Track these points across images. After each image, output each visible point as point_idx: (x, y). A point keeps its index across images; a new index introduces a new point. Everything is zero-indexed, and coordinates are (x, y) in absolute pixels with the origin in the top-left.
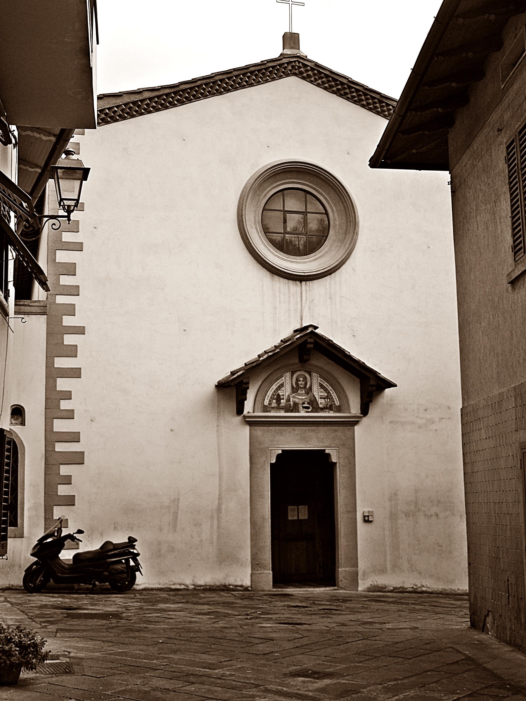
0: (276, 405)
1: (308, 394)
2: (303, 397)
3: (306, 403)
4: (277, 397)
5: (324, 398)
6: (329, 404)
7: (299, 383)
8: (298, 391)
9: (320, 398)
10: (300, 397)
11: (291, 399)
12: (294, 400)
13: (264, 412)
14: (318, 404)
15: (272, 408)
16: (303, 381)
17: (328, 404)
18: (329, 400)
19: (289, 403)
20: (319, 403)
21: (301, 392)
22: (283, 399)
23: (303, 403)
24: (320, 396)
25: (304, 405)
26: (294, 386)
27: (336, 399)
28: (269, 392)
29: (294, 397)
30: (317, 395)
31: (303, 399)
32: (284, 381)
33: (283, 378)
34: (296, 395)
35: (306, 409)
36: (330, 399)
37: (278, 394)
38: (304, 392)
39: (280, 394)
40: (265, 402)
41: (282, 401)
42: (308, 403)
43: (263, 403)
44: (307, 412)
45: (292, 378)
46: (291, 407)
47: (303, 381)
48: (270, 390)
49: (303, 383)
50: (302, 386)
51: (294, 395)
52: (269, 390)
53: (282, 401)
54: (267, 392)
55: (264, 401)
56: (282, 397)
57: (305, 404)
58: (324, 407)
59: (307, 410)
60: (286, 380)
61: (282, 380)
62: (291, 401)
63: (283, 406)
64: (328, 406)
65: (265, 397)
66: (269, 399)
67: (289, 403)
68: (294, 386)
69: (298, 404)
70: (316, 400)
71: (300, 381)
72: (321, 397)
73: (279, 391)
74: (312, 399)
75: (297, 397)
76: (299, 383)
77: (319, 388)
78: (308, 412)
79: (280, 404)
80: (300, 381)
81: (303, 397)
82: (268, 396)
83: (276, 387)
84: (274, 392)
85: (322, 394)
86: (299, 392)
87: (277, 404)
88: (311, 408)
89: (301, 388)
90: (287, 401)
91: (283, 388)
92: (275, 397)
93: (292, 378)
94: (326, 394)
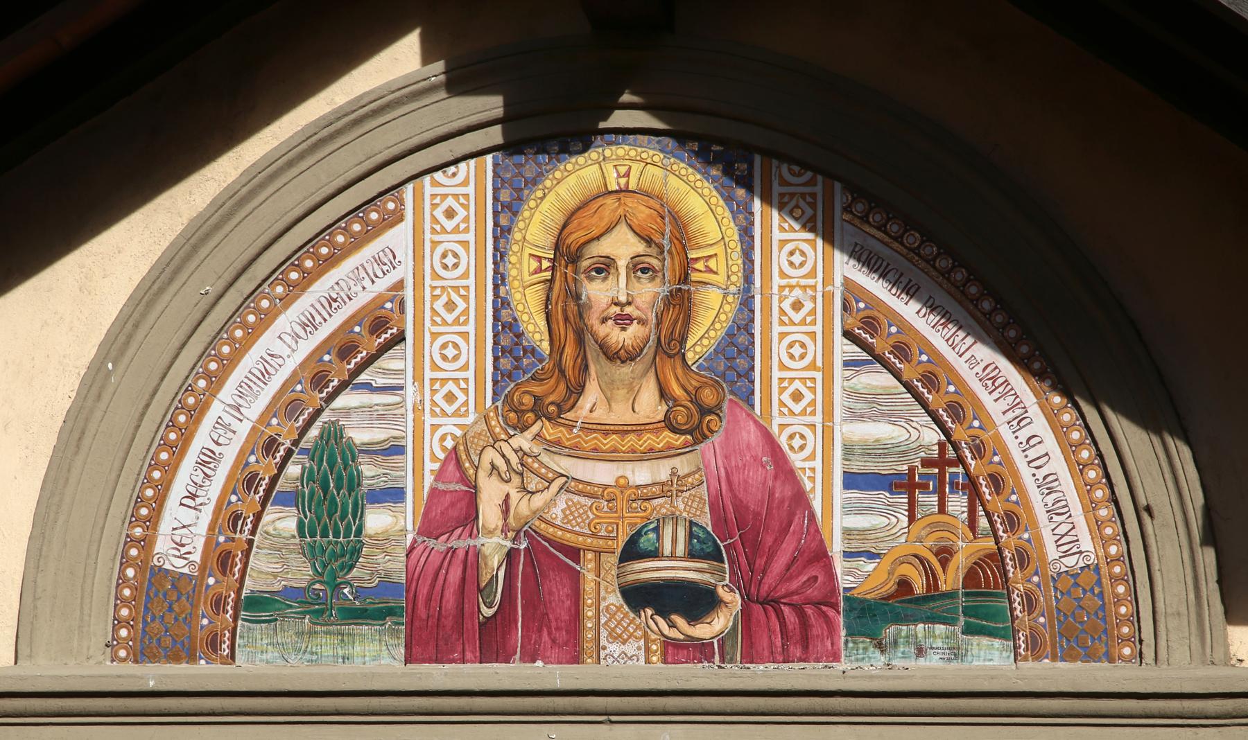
0: (300, 573)
1: (698, 434)
2: (641, 474)
3: (674, 540)
4: (308, 476)
5: (906, 485)
6: (965, 552)
7: (598, 292)
8: (577, 390)
9: (852, 481)
10: (602, 473)
11: (491, 494)
12: (523, 506)
13: (141, 654)
14: (821, 556)
15: (258, 604)
16: (638, 268)
17: (944, 555)
18: (958, 504)
19: (461, 543)
20: (836, 547)
21: (620, 414)
22: (394, 495)
23: (632, 552)
24: (849, 450)
25: (647, 571)
26: (535, 329)
27: (1048, 485)
28: (216, 409)
29: (524, 466)
30: (814, 441)
31: (643, 495)
32: (404, 271)
33: (399, 238)
34: (554, 446)
35: (663, 612)
36: (972, 488)
37: (333, 435)
38: (649, 406)
39: (359, 435)
40: (165, 526)
41: (376, 520)
42: (702, 549)
43: (146, 544)
44: (674, 650)
45: (502, 233)
46: (485, 591)
47: (638, 268)
48: (228, 392)
49: (648, 292)
50: (628, 336)
51: (523, 441)
52: (216, 382)
53: (376, 520)
54: (201, 409)
55: (153, 521)
56: (368, 470)
57: (655, 554)
58: (904, 585)
59: (682, 628)
60: (432, 260)
61: (388, 261)
62: (489, 513)
63: (387, 585)
64: (950, 580)
65: (171, 470)
66: (214, 490)
67: (461, 543)
68: (535, 329)
69: (574, 553)
70: (800, 498)
71: (605, 267)
72: (856, 466)
73: (346, 400)
74: (753, 498)
75: (564, 464)
76: (598, 292)
77: (844, 349)
78: (700, 651)
79: (356, 552)
80: (605, 267)
81: (641, 474)
82: (208, 461)
83: (306, 347)
84: (286, 405)
85: (882, 431)
86: (591, 401)
87: (312, 553)
88: (733, 600)
89: (614, 355)
90: (429, 528)
91: (389, 362)
92: (293, 470)
93: (502, 233)
94: (932, 436)
